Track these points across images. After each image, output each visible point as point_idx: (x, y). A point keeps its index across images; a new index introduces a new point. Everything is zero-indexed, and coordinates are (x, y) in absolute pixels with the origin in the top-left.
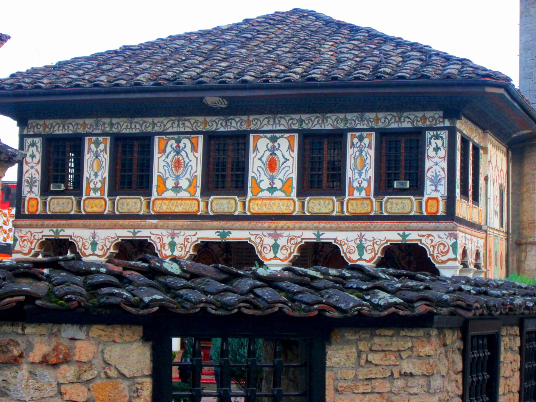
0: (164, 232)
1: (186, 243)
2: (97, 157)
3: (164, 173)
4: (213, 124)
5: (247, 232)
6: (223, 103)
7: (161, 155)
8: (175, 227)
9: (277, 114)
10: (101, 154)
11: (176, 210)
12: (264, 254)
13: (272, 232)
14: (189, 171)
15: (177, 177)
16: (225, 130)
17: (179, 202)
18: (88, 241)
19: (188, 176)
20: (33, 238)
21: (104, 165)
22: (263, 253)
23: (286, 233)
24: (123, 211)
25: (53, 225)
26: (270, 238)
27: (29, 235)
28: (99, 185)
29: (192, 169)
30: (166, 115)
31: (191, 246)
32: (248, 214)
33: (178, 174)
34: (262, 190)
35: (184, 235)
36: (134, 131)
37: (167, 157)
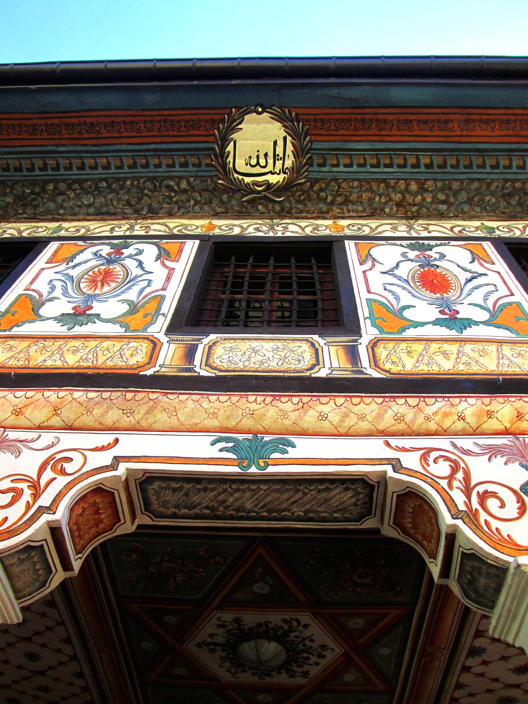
3: (45, 290)
6: (279, 163)
8: (18, 412)
9: (416, 217)
11: (49, 363)
12: (494, 524)
14: (136, 289)
16: (267, 235)
22: (483, 516)
26: (499, 460)
29: (149, 285)
30: (102, 214)
31: (69, 486)
32: (375, 374)
33: (97, 292)
35: (53, 445)
37: (74, 267)
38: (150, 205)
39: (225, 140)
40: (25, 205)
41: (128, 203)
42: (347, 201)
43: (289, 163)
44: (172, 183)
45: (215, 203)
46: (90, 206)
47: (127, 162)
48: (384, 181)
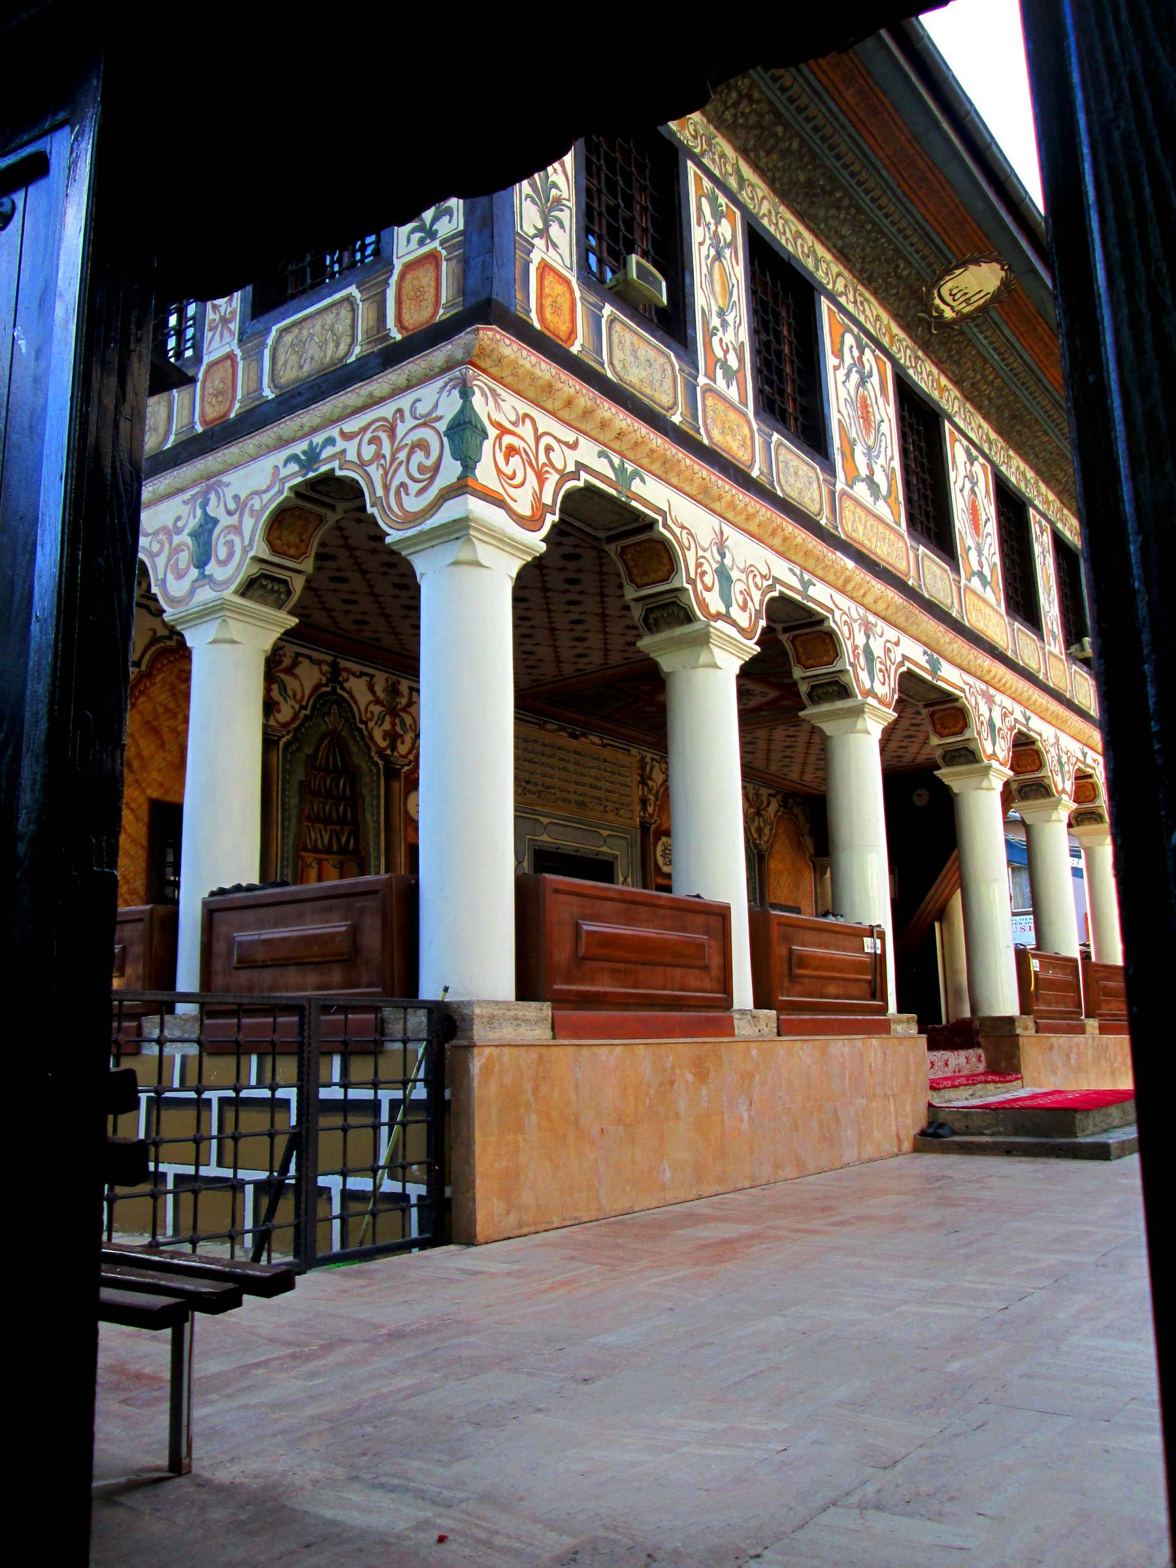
0: (856, 611)
1: (888, 663)
2: (719, 256)
4: (899, 351)
5: (957, 671)
7: (836, 362)
10: (727, 252)
13: (984, 687)
14: (883, 450)
15: (869, 449)
17: (881, 528)
18: (707, 555)
19: (882, 461)
20: (542, 459)
21: (735, 298)
23: (999, 697)
24: (788, 490)
25: (620, 436)
27: (526, 430)
28: (733, 362)
30: (843, 255)
34: (973, 574)
36: (783, 242)
37: (848, 375)
38: (872, 273)
39: (964, 264)
40: (807, 195)
41: (864, 259)
42: (957, 363)
43: (965, 311)
44: (902, 265)
45: (904, 303)
46: (842, 237)
47: (903, 224)
48: (985, 361)
